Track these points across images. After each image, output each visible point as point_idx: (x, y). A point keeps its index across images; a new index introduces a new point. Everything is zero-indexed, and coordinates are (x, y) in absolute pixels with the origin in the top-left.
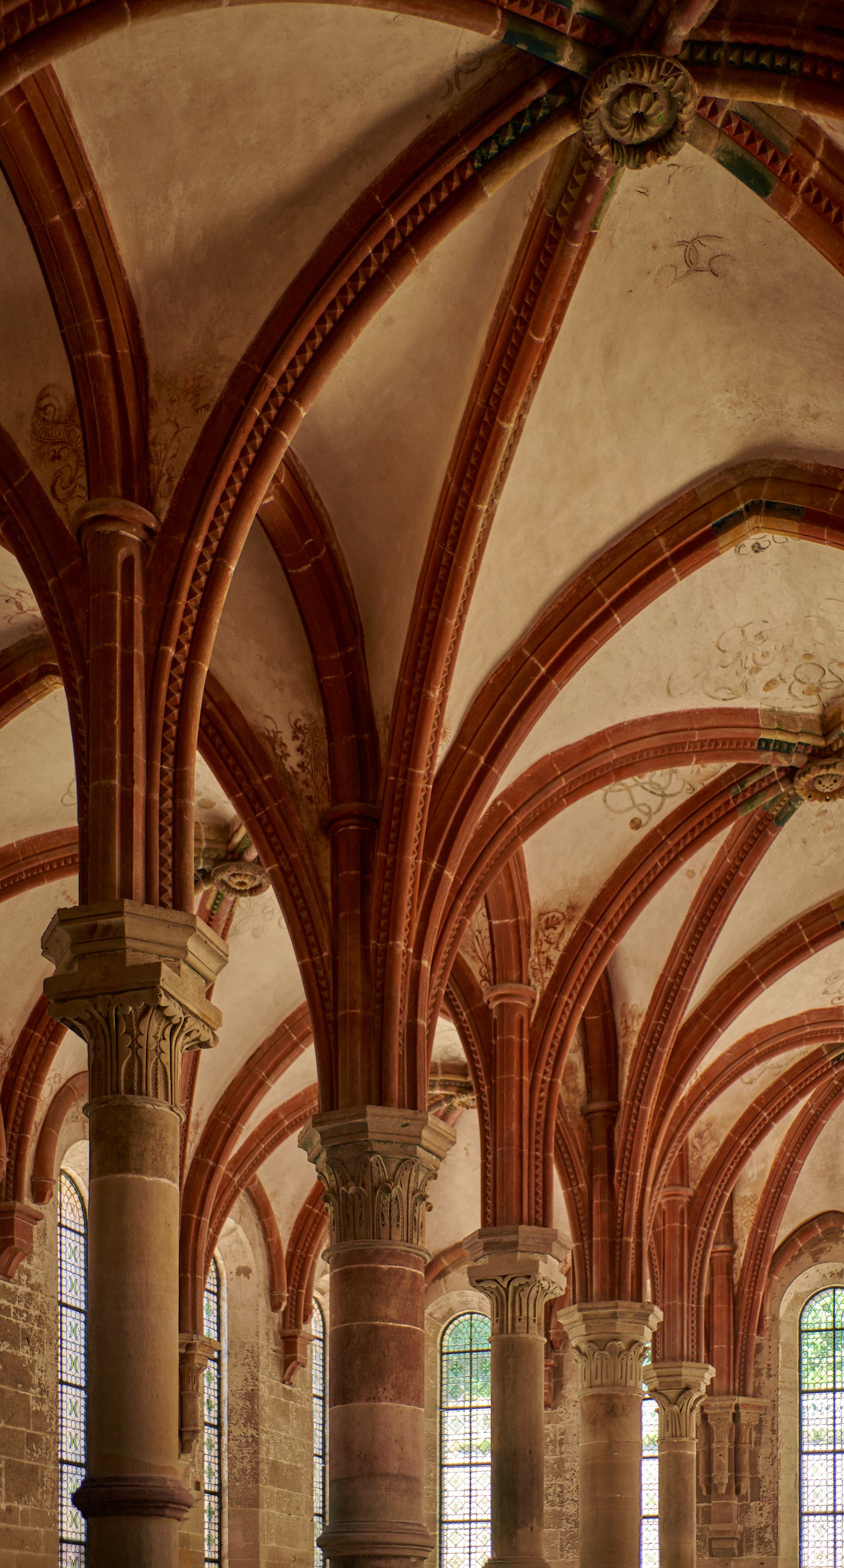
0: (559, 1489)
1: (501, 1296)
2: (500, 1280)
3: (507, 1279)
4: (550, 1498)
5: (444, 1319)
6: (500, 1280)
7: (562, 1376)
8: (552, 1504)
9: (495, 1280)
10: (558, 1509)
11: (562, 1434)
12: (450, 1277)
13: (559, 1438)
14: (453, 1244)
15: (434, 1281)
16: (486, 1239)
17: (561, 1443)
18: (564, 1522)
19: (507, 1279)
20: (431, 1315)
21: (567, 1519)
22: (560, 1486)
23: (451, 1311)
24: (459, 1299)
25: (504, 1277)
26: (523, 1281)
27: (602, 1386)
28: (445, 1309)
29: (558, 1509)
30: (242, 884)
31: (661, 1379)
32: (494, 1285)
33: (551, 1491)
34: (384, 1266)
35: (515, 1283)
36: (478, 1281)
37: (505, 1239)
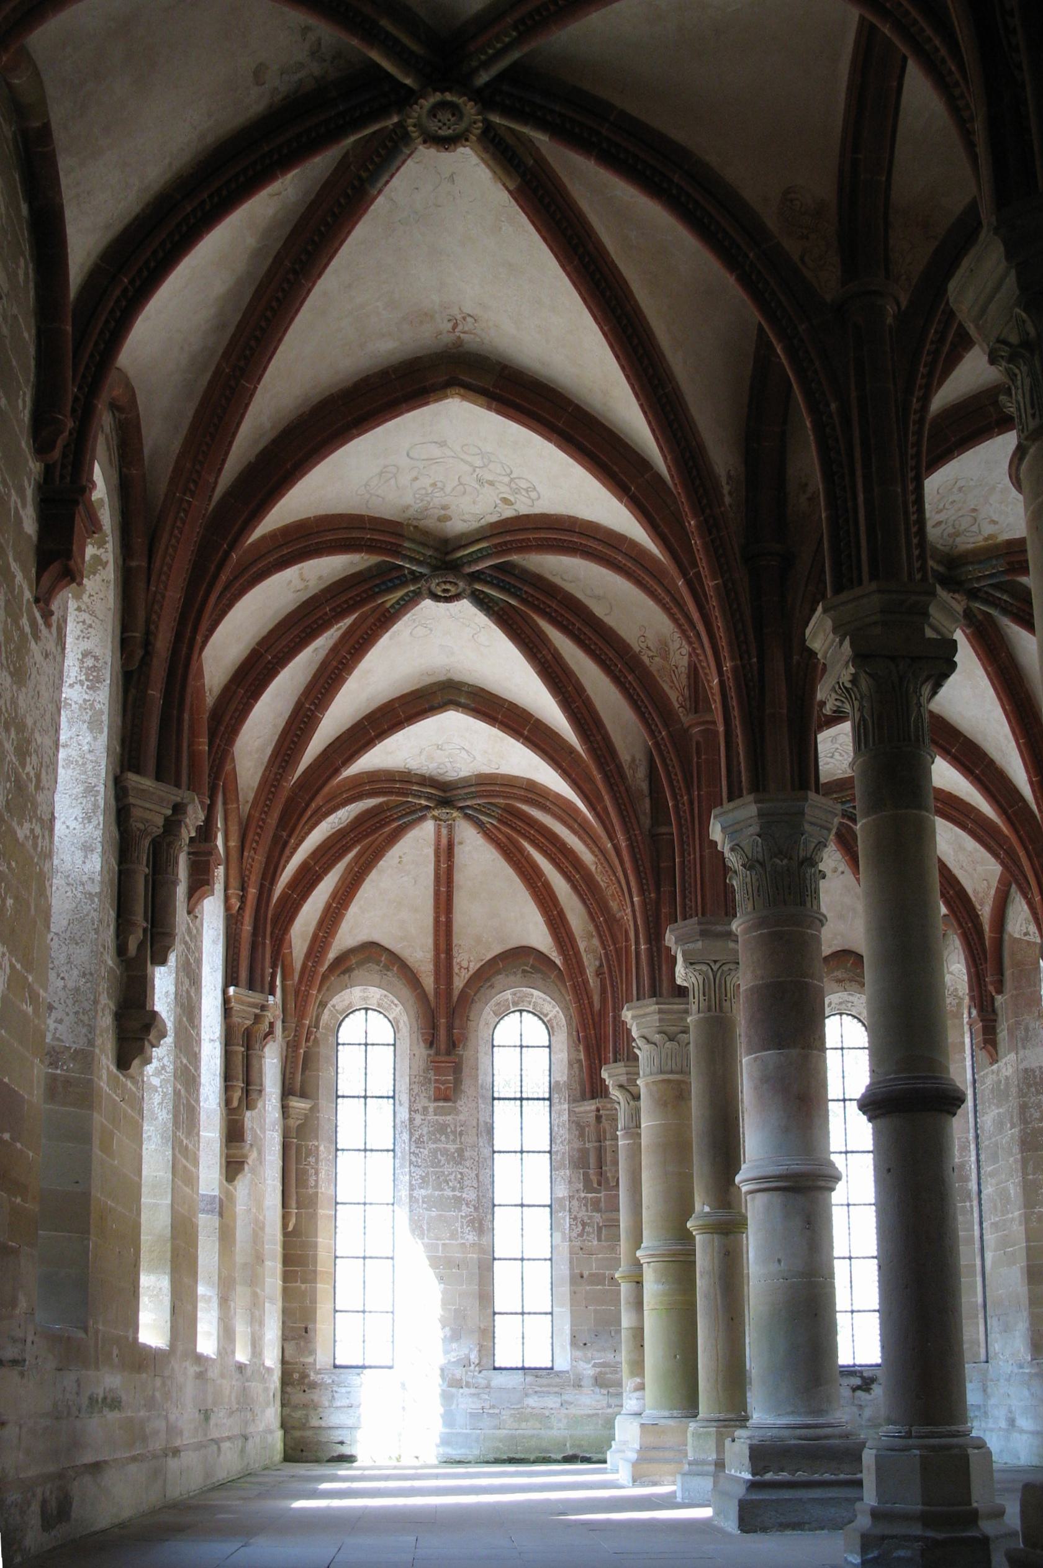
0: (459, 1176)
1: (709, 979)
2: (712, 964)
3: (718, 965)
4: (450, 1184)
5: (344, 1011)
6: (712, 964)
7: (461, 1072)
8: (454, 1189)
9: (708, 964)
10: (459, 1194)
12: (356, 972)
13: (459, 1130)
14: (360, 943)
15: (338, 976)
16: (703, 927)
17: (461, 1134)
18: (464, 1207)
19: (718, 965)
20: (334, 1006)
21: (467, 1205)
22: (461, 1173)
23: (350, 1005)
24: (361, 994)
25: (715, 962)
26: (733, 966)
27: (672, 1072)
28: (346, 1003)
29: (458, 1194)
30: (445, 591)
31: (629, 1076)
32: (704, 968)
33: (452, 1177)
34: (809, 931)
35: (725, 968)
36: (691, 964)
37: (719, 928)
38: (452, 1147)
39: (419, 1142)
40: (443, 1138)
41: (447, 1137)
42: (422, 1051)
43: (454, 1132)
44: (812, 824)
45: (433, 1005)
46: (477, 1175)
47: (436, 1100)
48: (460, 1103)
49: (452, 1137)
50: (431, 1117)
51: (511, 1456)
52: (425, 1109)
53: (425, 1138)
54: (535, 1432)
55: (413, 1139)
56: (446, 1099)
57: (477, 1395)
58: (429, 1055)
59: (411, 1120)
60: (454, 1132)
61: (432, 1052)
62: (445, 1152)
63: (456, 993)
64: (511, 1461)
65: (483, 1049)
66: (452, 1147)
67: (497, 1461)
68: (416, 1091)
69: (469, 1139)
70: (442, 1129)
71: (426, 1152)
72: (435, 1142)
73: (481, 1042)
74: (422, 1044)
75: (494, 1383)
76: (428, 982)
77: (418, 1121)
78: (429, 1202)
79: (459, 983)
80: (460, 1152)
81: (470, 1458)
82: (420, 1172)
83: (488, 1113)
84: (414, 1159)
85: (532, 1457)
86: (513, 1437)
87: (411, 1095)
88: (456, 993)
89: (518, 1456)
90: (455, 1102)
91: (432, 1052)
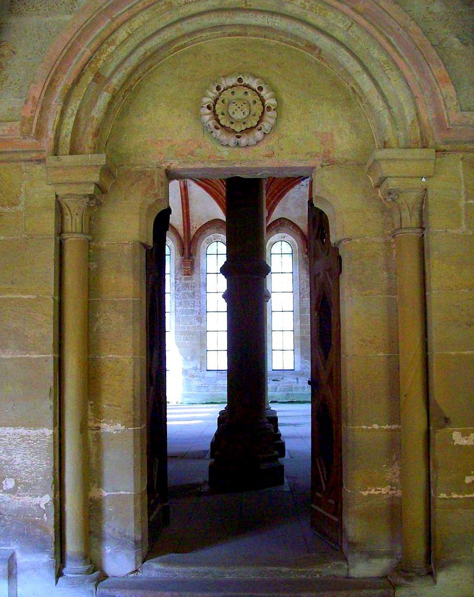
11: (194, 284)
17: (194, 287)
18: (195, 313)
38: (190, 292)
39: (178, 290)
40: (187, 288)
41: (189, 288)
42: (179, 257)
43: (191, 286)
44: (303, 173)
45: (183, 241)
46: (200, 302)
47: (184, 275)
48: (193, 276)
49: (190, 288)
50: (183, 281)
51: (212, 401)
52: (180, 278)
53: (181, 289)
54: (221, 393)
55: (176, 289)
56: (188, 275)
57: (200, 380)
58: (182, 259)
59: (175, 282)
60: (191, 286)
61: (183, 258)
62: (188, 294)
63: (192, 236)
64: (212, 403)
65: (202, 256)
66: (190, 292)
67: (207, 403)
68: (177, 272)
69: (197, 289)
70: (187, 285)
71: (181, 294)
72: (184, 290)
73: (201, 254)
74: (180, 255)
75: (206, 376)
76: (181, 232)
77: (178, 283)
78: (182, 312)
79: (193, 233)
80: (194, 293)
81: (197, 402)
82: (178, 301)
83: (205, 279)
84: (176, 296)
85: (219, 402)
86: (212, 395)
87: (175, 273)
88: (192, 236)
89: (214, 401)
90: (192, 276)
91: (183, 258)
